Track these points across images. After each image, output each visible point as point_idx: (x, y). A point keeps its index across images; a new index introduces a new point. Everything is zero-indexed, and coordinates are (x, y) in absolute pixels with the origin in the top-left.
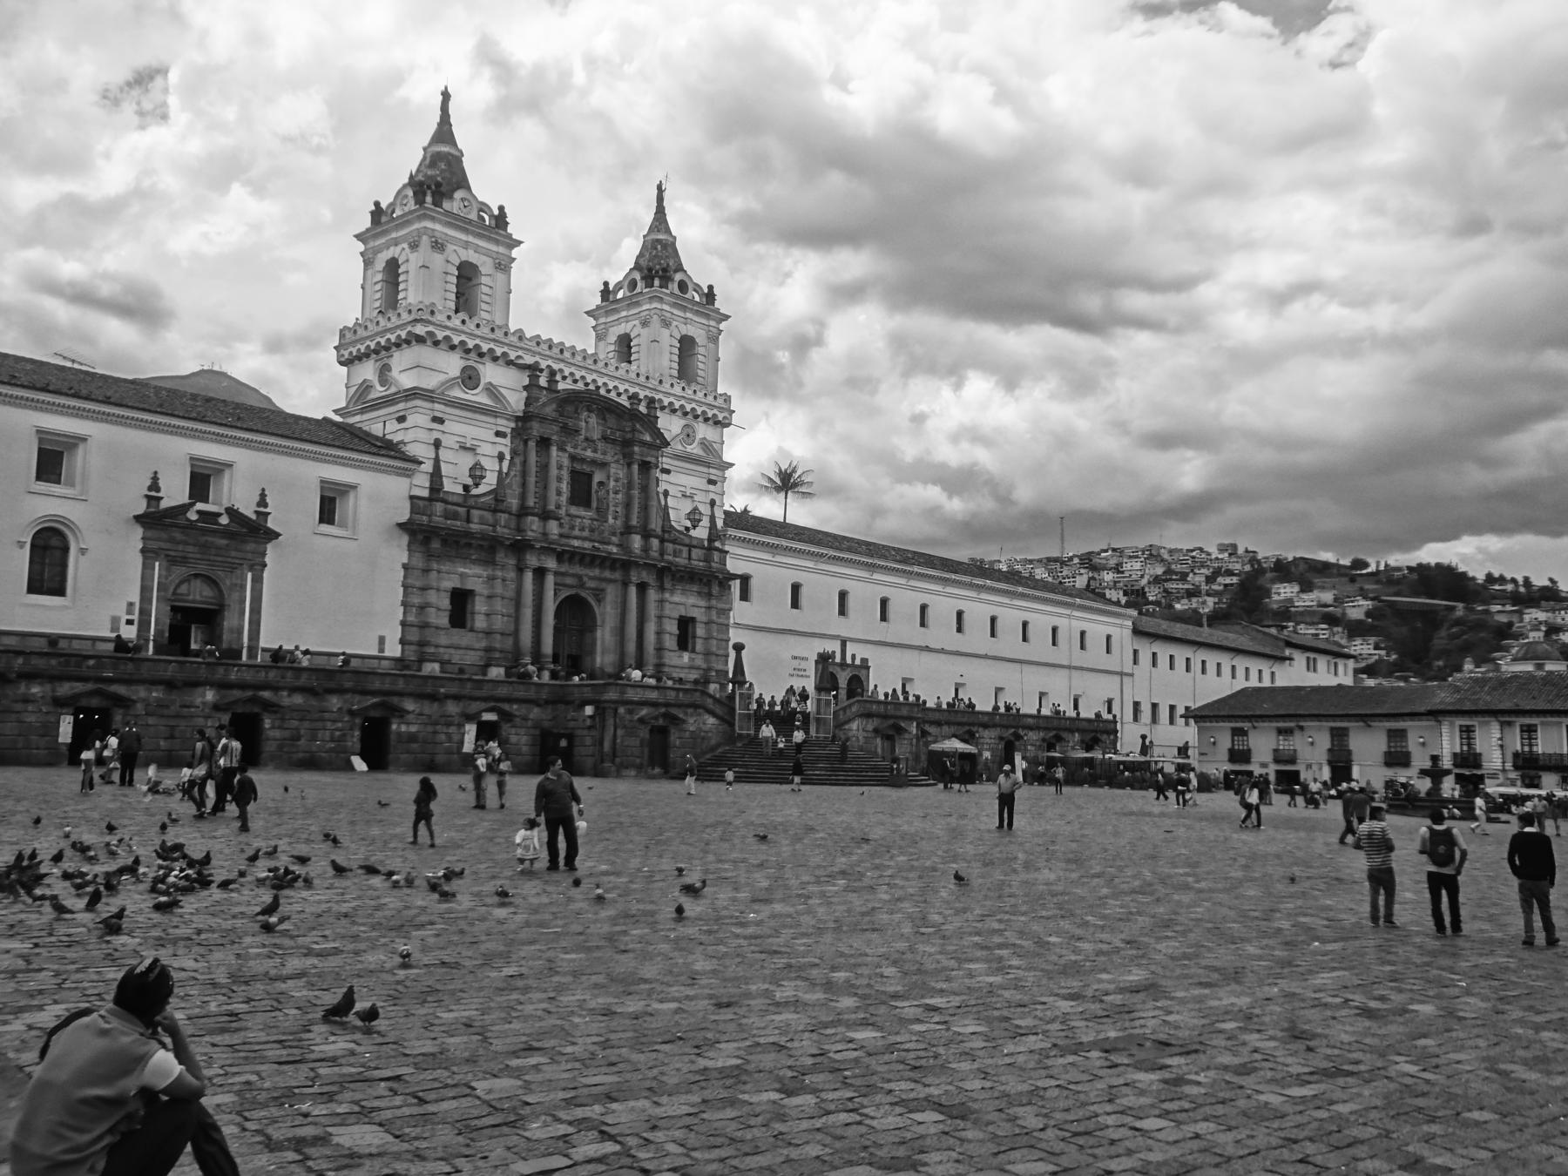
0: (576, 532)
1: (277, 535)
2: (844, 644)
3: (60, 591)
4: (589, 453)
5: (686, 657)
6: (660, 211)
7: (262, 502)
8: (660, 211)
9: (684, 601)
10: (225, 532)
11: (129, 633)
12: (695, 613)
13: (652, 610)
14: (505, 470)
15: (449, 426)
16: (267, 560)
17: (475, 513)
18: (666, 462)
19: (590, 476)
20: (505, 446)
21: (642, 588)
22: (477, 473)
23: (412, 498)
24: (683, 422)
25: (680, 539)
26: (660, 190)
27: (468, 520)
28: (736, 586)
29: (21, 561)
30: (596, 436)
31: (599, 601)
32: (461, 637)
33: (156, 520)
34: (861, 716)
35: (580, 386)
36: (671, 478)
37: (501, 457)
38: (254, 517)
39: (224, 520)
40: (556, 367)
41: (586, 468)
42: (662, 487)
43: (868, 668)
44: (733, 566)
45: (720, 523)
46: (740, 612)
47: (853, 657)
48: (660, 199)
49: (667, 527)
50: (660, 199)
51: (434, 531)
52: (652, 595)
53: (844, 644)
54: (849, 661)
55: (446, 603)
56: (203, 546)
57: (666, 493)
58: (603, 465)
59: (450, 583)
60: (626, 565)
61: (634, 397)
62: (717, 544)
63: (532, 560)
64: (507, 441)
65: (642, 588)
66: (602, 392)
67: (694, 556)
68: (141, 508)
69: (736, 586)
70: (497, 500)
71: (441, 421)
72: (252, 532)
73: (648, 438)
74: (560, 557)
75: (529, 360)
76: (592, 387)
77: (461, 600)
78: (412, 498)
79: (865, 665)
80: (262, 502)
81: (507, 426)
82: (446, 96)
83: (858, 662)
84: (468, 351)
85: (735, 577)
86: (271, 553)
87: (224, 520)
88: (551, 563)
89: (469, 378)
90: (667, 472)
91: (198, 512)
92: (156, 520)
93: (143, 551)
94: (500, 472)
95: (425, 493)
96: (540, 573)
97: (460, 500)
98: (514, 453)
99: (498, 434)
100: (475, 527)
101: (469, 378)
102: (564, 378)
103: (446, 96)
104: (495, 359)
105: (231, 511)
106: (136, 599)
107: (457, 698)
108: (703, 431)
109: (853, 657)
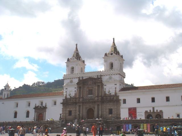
0: (88, 99)
1: (47, 108)
2: (153, 108)
3: (28, 117)
4: (90, 87)
5: (110, 115)
6: (114, 42)
7: (46, 104)
8: (114, 42)
9: (109, 106)
10: (42, 109)
11: (33, 121)
12: (112, 108)
13: (100, 109)
14: (76, 93)
15: (68, 89)
16: (47, 111)
17: (71, 100)
18: (105, 84)
19: (92, 89)
20: (76, 89)
21: (98, 105)
22: (70, 95)
23: (63, 99)
24: (109, 76)
25: (110, 95)
26: (114, 39)
27: (70, 101)
28: (122, 102)
29: (25, 115)
30: (91, 84)
31: (94, 108)
32: (71, 117)
33: (36, 108)
34: (86, 123)
35: (88, 77)
36: (107, 86)
37: (75, 91)
38: (45, 106)
39: (42, 107)
40: (83, 76)
41: (91, 89)
42: (104, 88)
43: (163, 112)
44: (120, 98)
45: (117, 92)
46: (122, 105)
47: (157, 110)
48: (114, 40)
49: (105, 94)
50: (114, 40)
51: (66, 103)
52: (100, 106)
53: (153, 108)
54: (155, 111)
55: (67, 112)
56: (41, 110)
57: (105, 89)
58: (93, 87)
59: (69, 110)
60: (95, 102)
61: (97, 76)
62: (117, 95)
63: (78, 105)
64: (77, 88)
65: (98, 105)
66: (92, 77)
67: (111, 98)
68: (34, 107)
69: (122, 102)
70: (75, 98)
71: (66, 89)
72: (45, 108)
73: (99, 81)
74: (83, 103)
75: (78, 77)
76: (90, 77)
77: (70, 113)
78: (63, 99)
79: (161, 111)
80: (46, 104)
81: (76, 86)
82: (77, 45)
83: (159, 111)
84: (70, 79)
85: (121, 100)
86: (47, 109)
87: (42, 107)
88: (81, 105)
89: (71, 82)
90: (106, 85)
91: (40, 107)
92: (36, 108)
93: (35, 112)
94: (75, 93)
95: (65, 99)
96: (80, 106)
98: (77, 90)
99: (75, 88)
100: (71, 102)
101: (71, 82)
102: (85, 77)
103: (77, 45)
104: (74, 78)
105: (43, 106)
106: (34, 117)
107: (32, 125)
108: (113, 76)
109: (157, 110)
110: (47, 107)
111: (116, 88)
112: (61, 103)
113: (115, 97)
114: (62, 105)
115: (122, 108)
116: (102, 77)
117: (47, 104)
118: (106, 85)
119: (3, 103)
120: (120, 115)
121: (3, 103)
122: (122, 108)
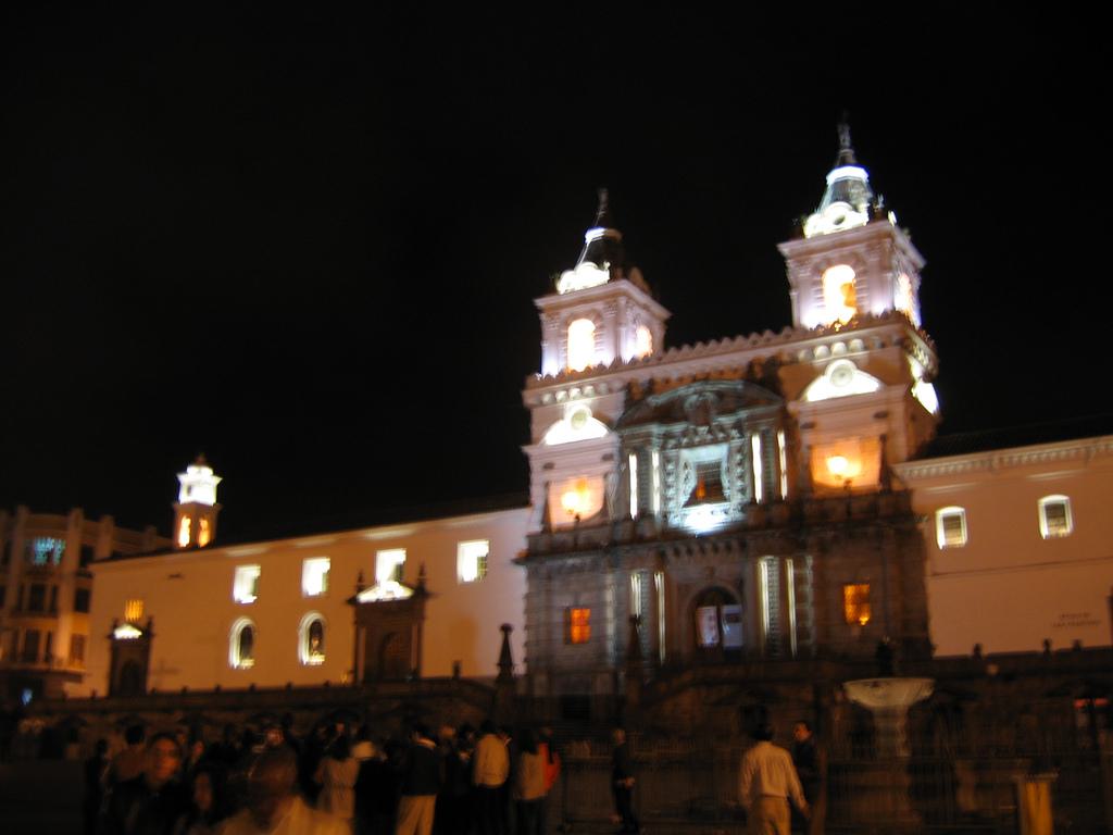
7: (422, 572)
64: (616, 458)
80: (422, 572)
90: (811, 426)
97: (572, 525)
110: (429, 587)
111: (884, 439)
112: (518, 562)
113: (882, 502)
114: (521, 573)
115: (935, 574)
116: (782, 373)
117: (428, 570)
118: (811, 426)
119: (178, 576)
120: (924, 626)
121: (178, 576)
122: (935, 574)
